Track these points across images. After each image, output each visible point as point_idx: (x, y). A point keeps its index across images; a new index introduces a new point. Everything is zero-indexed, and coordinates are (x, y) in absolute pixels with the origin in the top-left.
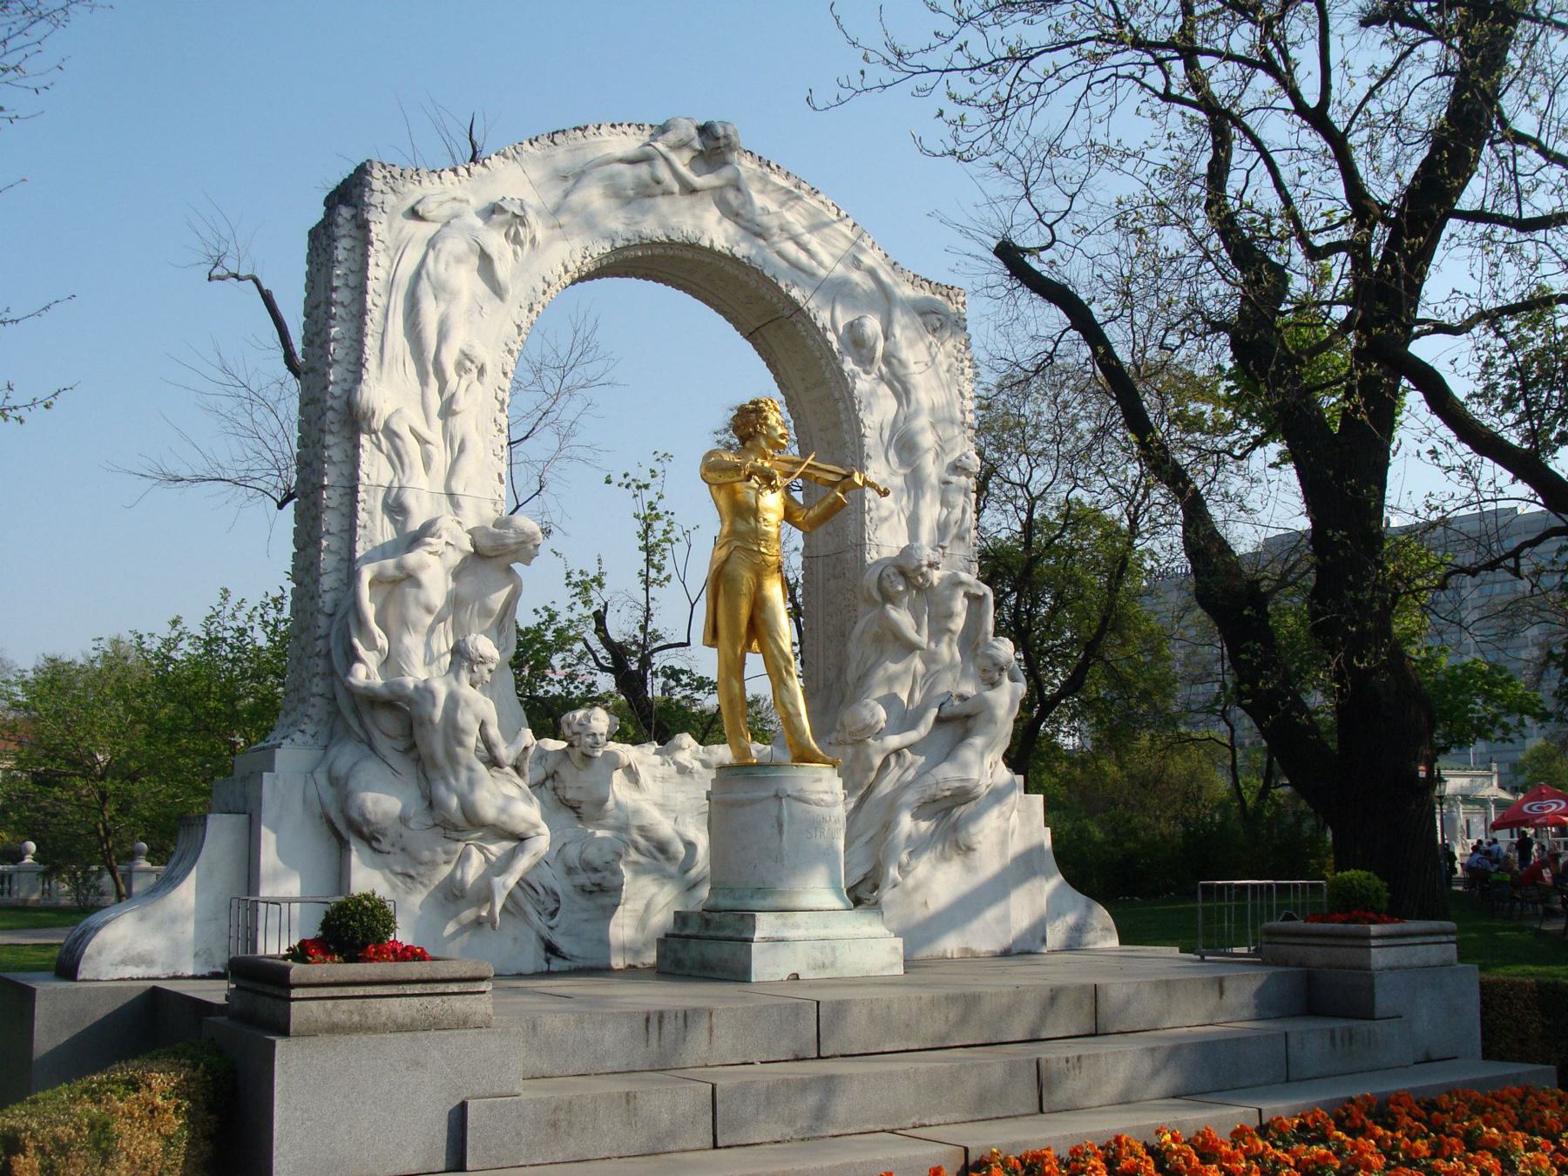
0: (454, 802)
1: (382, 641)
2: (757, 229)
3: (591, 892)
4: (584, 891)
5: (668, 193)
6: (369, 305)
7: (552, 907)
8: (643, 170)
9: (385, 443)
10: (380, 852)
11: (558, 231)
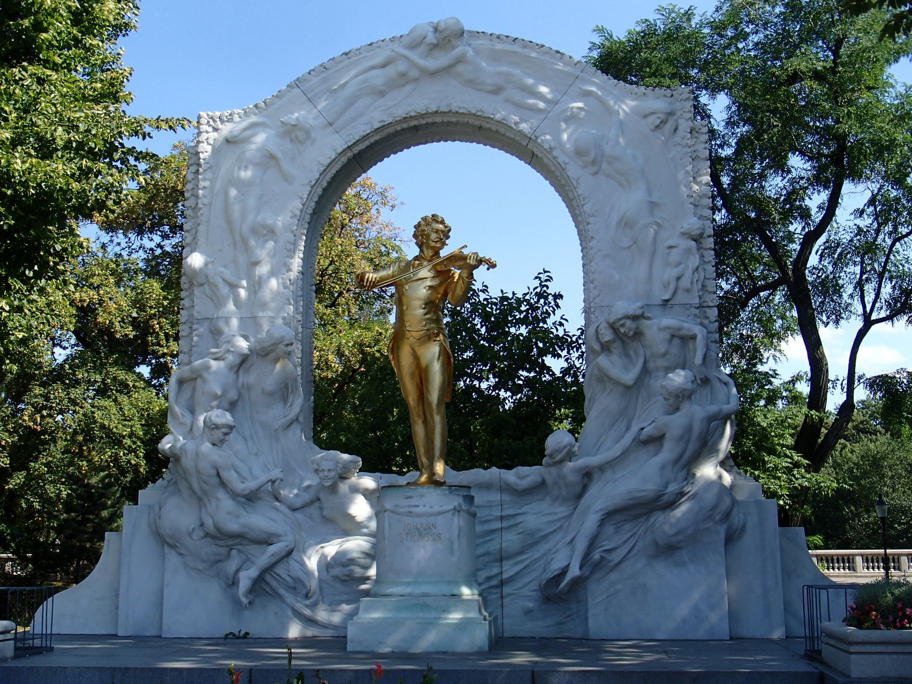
0: (209, 522)
1: (188, 419)
2: (488, 88)
3: (345, 581)
4: (336, 578)
5: (416, 80)
6: (200, 205)
7: (304, 592)
8: (391, 71)
9: (208, 292)
10: (181, 554)
11: (331, 129)
